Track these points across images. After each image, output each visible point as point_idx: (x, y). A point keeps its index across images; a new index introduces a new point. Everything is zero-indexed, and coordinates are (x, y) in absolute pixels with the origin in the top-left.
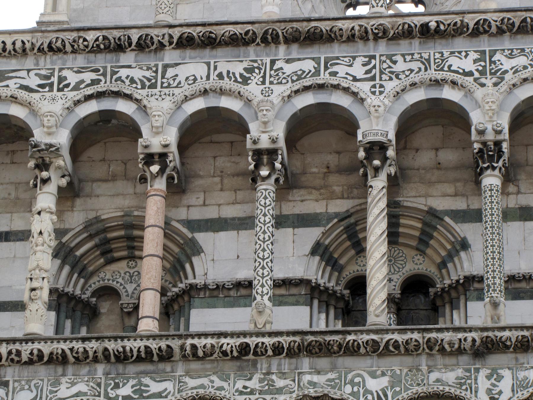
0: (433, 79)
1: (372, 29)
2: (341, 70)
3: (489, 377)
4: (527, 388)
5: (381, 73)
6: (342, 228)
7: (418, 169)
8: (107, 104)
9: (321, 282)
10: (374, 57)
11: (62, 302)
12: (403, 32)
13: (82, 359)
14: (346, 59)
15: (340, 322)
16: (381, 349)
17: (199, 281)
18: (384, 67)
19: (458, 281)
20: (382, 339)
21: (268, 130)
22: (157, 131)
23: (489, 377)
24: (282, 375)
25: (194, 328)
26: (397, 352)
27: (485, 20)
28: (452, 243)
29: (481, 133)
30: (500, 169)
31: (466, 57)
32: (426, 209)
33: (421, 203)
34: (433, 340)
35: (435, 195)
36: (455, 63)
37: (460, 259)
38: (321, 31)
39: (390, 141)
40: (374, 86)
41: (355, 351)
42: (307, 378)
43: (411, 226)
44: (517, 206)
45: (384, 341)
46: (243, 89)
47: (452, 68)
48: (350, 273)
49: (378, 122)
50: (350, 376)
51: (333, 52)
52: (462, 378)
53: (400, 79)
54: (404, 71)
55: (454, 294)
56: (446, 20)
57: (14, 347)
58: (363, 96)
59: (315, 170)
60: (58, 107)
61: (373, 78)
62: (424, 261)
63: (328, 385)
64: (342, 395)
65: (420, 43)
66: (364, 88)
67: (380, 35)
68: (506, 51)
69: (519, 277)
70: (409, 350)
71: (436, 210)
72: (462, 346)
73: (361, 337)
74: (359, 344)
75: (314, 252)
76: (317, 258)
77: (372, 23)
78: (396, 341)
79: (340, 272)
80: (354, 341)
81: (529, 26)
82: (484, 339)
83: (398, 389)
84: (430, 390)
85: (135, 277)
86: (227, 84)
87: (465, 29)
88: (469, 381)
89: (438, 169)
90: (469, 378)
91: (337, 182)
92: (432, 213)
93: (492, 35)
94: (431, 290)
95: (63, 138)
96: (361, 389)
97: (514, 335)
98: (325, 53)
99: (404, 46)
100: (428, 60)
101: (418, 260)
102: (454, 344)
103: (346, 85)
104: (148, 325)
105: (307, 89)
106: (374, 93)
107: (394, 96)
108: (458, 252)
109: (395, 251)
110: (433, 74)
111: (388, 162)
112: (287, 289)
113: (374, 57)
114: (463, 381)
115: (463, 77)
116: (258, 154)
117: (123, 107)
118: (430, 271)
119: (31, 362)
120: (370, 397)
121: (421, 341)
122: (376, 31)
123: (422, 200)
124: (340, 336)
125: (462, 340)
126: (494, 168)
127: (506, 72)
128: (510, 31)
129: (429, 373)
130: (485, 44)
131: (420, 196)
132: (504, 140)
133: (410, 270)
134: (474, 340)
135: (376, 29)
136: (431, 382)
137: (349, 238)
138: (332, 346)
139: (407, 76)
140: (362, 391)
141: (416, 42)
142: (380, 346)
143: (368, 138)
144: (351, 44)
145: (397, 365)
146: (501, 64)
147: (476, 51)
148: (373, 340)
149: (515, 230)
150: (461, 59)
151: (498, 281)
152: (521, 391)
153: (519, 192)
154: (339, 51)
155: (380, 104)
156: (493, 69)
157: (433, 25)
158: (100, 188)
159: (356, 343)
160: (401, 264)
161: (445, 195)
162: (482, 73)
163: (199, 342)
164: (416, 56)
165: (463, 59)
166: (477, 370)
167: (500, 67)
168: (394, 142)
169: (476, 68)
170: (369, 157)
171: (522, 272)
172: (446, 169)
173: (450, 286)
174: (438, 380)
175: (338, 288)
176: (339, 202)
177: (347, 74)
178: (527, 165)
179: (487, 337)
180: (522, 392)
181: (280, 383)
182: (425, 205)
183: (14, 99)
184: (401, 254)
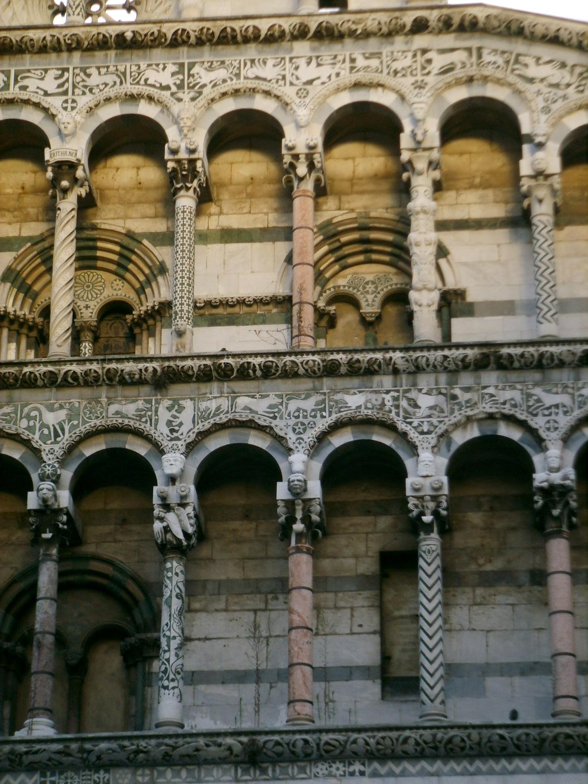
0: (129, 93)
1: (65, 40)
2: (32, 83)
3: (169, 409)
4: (209, 419)
5: (74, 87)
6: (35, 253)
7: (118, 190)
9: (10, 309)
10: (67, 70)
12: (98, 43)
14: (38, 72)
15: (33, 352)
16: (59, 380)
18: (78, 81)
19: (153, 307)
20: (59, 371)
23: (169, 409)
26: (76, 384)
27: (184, 30)
28: (150, 268)
29: (174, 152)
30: (195, 189)
31: (164, 69)
32: (124, 231)
33: (119, 226)
34: (112, 371)
35: (134, 216)
36: (153, 76)
37: (157, 283)
38: (11, 40)
39: (79, 160)
40: (66, 101)
41: (33, 384)
43: (108, 250)
44: (218, 228)
45: (63, 372)
47: (149, 82)
48: (45, 300)
50: (26, 410)
51: (24, 65)
52: (142, 410)
53: (94, 94)
54: (98, 86)
55: (151, 322)
56: (143, 30)
58: (55, 113)
59: (9, 191)
61: (65, 93)
62: (123, 287)
63: (3, 420)
64: (17, 429)
65: (116, 54)
66: (55, 103)
67: (74, 46)
68: (206, 63)
69: (216, 302)
70: (89, 381)
71: (134, 233)
72: (143, 377)
73: (38, 368)
74: (35, 375)
76: (8, 285)
77: (64, 33)
78: (74, 372)
79: (34, 299)
80: (31, 373)
81: (229, 36)
82: (166, 369)
83: (75, 422)
84: (109, 423)
87: (163, 40)
88: (149, 413)
89: (140, 189)
90: (150, 410)
92: (130, 235)
93: (191, 46)
94: (127, 316)
96: (37, 423)
97: (195, 364)
98: (16, 65)
100: (124, 74)
101: (118, 285)
102: (135, 374)
103: (37, 101)
106: (65, 109)
107: (87, 112)
108: (155, 276)
109: (93, 276)
110: (130, 88)
111: (79, 183)
113: (67, 70)
114: (143, 413)
115: (159, 91)
118: (129, 297)
120: (46, 432)
121: (100, 372)
122: (69, 42)
123: (120, 222)
124: (17, 368)
125: (143, 371)
126: (188, 189)
127: (204, 86)
128: (210, 41)
129: (109, 405)
130: (184, 55)
131: (118, 218)
132: (199, 159)
133: (108, 296)
134: (155, 370)
135: (68, 39)
136: (110, 415)
137: (44, 262)
138: (8, 378)
139: (101, 91)
140: (38, 426)
141: (112, 53)
142: (58, 378)
143: (56, 158)
144: (43, 56)
145: (75, 397)
146: (200, 77)
147: (174, 64)
148: (51, 372)
149: (214, 252)
150: (158, 71)
151: (185, 308)
152: (202, 422)
153: (221, 213)
154: (31, 64)
155: (70, 121)
156: (191, 82)
157: (129, 35)
159: (32, 375)
160: (99, 290)
161: (144, 217)
162: (180, 87)
164: (112, 69)
165: (159, 71)
166: (158, 402)
167: (199, 80)
168: (84, 161)
169: (174, 82)
171: (219, 297)
172: (148, 189)
173: (146, 312)
174: (117, 413)
175: (29, 316)
176: (33, 225)
177: (38, 88)
178: (231, 184)
179: (169, 367)
180: (203, 424)
182: (123, 228)
184: (99, 280)
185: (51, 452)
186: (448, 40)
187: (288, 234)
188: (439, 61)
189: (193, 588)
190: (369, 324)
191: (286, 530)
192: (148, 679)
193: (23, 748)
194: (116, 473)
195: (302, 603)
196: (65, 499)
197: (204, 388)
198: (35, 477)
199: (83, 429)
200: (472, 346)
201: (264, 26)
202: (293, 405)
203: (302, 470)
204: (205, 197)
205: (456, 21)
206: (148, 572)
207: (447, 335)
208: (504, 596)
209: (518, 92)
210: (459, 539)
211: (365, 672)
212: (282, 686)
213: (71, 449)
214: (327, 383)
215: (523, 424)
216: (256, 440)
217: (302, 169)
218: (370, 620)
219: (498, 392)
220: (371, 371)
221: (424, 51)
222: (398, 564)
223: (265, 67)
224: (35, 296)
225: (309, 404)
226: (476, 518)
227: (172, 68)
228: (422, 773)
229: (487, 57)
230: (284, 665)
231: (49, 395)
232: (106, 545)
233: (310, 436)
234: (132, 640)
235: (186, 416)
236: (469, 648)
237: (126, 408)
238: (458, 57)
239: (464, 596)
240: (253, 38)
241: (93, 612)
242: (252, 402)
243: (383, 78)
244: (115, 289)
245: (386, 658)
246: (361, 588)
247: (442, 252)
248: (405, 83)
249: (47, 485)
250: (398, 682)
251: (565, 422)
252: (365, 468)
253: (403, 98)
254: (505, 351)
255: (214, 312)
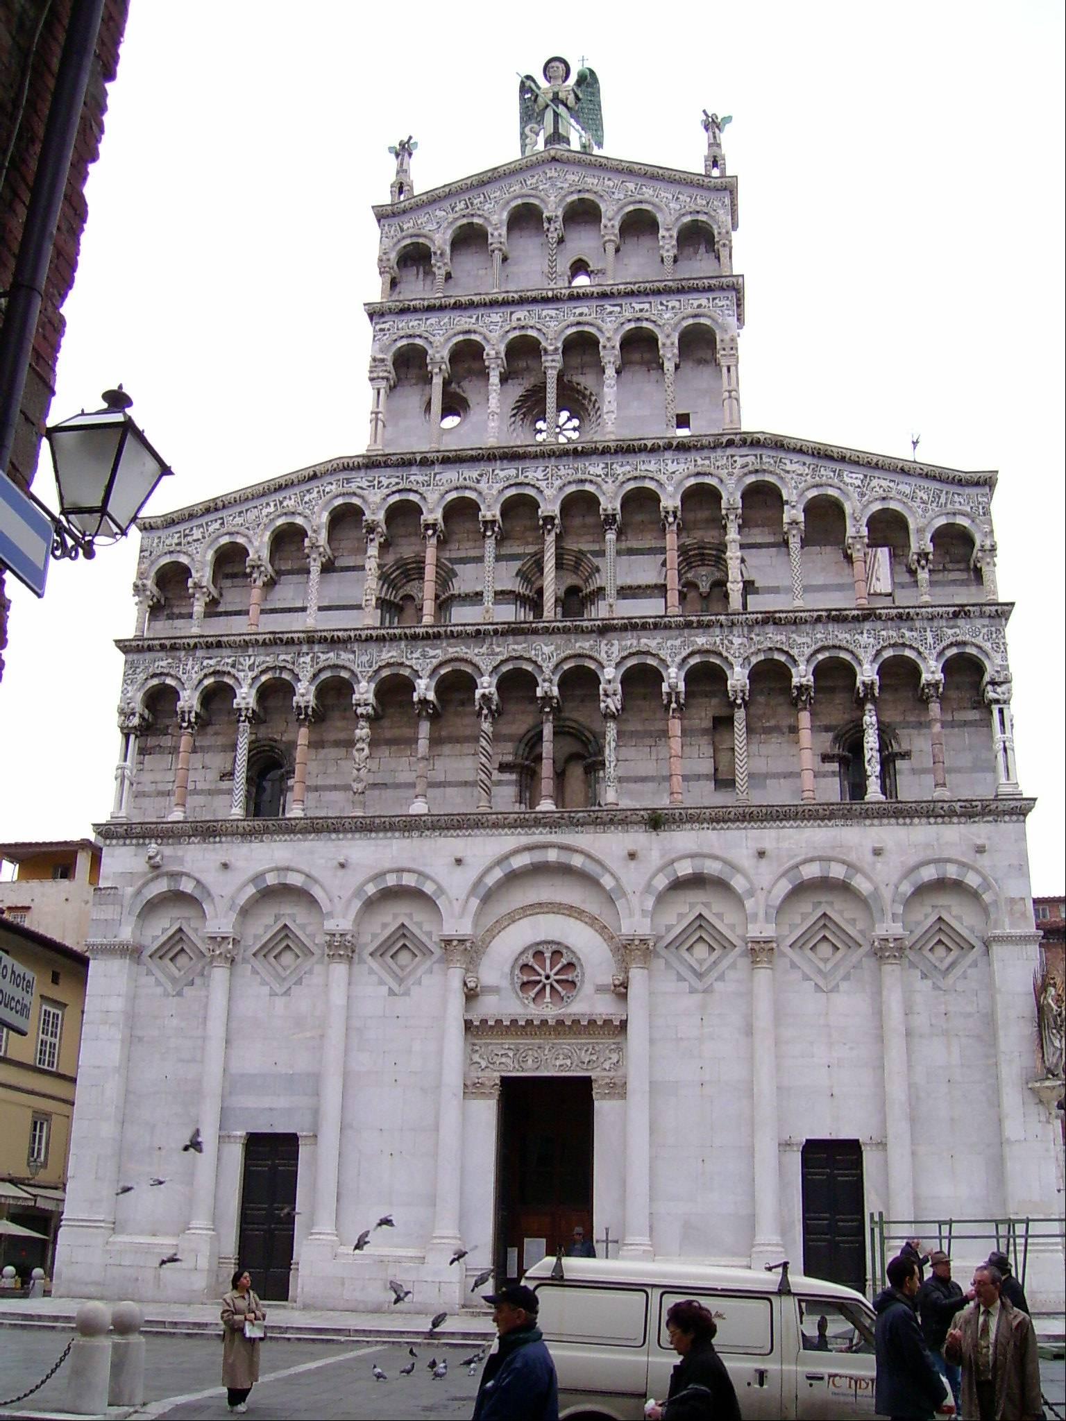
2: (530, 475)
8: (404, 496)
11: (383, 604)
13: (394, 638)
17: (456, 592)
21: (491, 511)
22: (431, 511)
24: (499, 646)
25: (453, 622)
29: (605, 510)
33: (575, 547)
36: (592, 470)
42: (511, 647)
43: (569, 559)
46: (478, 486)
49: (550, 506)
57: (358, 633)
60: (377, 499)
66: (542, 484)
70: (566, 631)
75: (517, 575)
85: (421, 590)
86: (468, 483)
91: (530, 537)
92: (581, 552)
95: (381, 516)
99: (564, 460)
104: (427, 619)
105: (511, 485)
110: (580, 476)
112: (502, 596)
116: (485, 522)
117: (413, 497)
119: (366, 640)
145: (559, 639)
158: (403, 541)
163: (455, 629)
165: (595, 468)
170: (545, 524)
181: (497, 650)
183: (354, 494)
185: (548, 667)
186: (744, 451)
187: (663, 551)
188: (740, 461)
189: (620, 734)
190: (705, 598)
191: (667, 707)
192: (597, 781)
193: (541, 816)
194: (580, 680)
195: (676, 744)
196: (555, 691)
197: (624, 634)
198: (540, 680)
199: (563, 655)
200: (761, 613)
201: (649, 443)
202: (669, 643)
203: (674, 677)
204: (620, 533)
205: (749, 441)
206: (596, 727)
207: (745, 605)
208: (775, 739)
209: (781, 478)
210: (752, 710)
211: (707, 777)
212: (666, 784)
213: (557, 666)
214: (686, 631)
215: (787, 653)
216: (651, 661)
217: (671, 519)
218: (709, 751)
219: (774, 637)
220: (709, 625)
221: (732, 456)
222: (723, 723)
223: (649, 465)
224: (534, 583)
225: (678, 642)
226: (761, 699)
227: (602, 465)
228: (738, 828)
229: (765, 460)
230: (665, 773)
231: (546, 638)
232: (578, 715)
233: (678, 659)
234: (589, 761)
235: (615, 649)
236: (760, 765)
237: (583, 645)
238: (751, 459)
239: (756, 738)
240: (643, 449)
241: (571, 746)
242: (649, 642)
243: (712, 470)
244: (571, 580)
245: (716, 770)
246: (703, 735)
247: (743, 561)
248: (723, 473)
249: (547, 684)
250: (724, 782)
251: (808, 651)
252: (707, 677)
253: (721, 481)
254: (777, 615)
255: (626, 592)
